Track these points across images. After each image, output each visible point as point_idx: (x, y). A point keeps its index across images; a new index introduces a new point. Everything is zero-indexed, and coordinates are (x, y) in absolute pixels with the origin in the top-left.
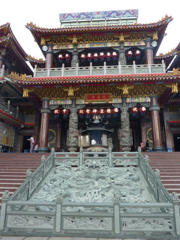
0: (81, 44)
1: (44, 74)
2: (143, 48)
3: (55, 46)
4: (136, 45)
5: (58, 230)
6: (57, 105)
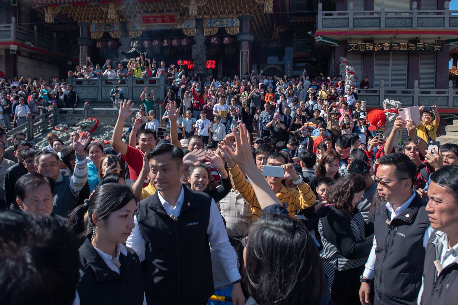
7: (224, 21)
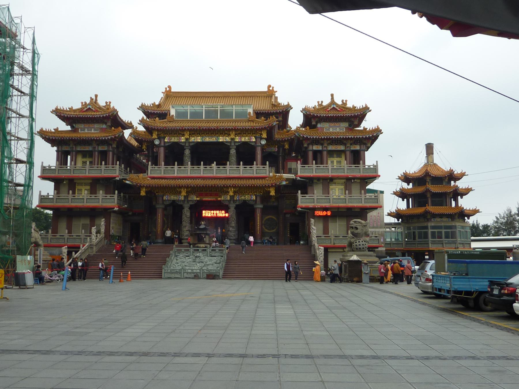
0: (193, 137)
1: (158, 171)
2: (253, 144)
3: (167, 137)
4: (247, 141)
5: (182, 277)
6: (171, 200)
7: (246, 196)
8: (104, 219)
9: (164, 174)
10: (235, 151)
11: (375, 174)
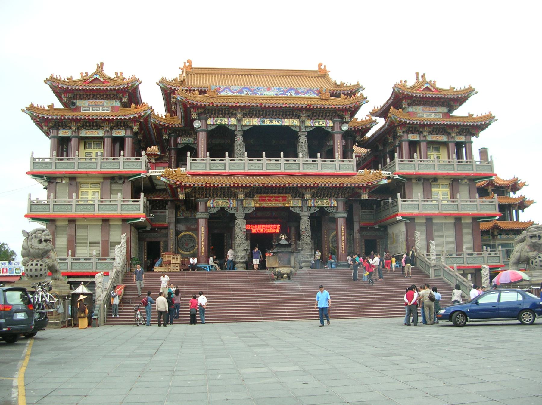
0: (248, 118)
1: (201, 165)
6: (217, 207)
8: (125, 234)
9: (210, 169)
10: (306, 140)
11: (490, 172)
